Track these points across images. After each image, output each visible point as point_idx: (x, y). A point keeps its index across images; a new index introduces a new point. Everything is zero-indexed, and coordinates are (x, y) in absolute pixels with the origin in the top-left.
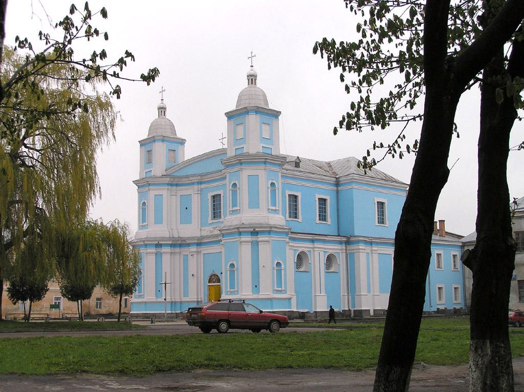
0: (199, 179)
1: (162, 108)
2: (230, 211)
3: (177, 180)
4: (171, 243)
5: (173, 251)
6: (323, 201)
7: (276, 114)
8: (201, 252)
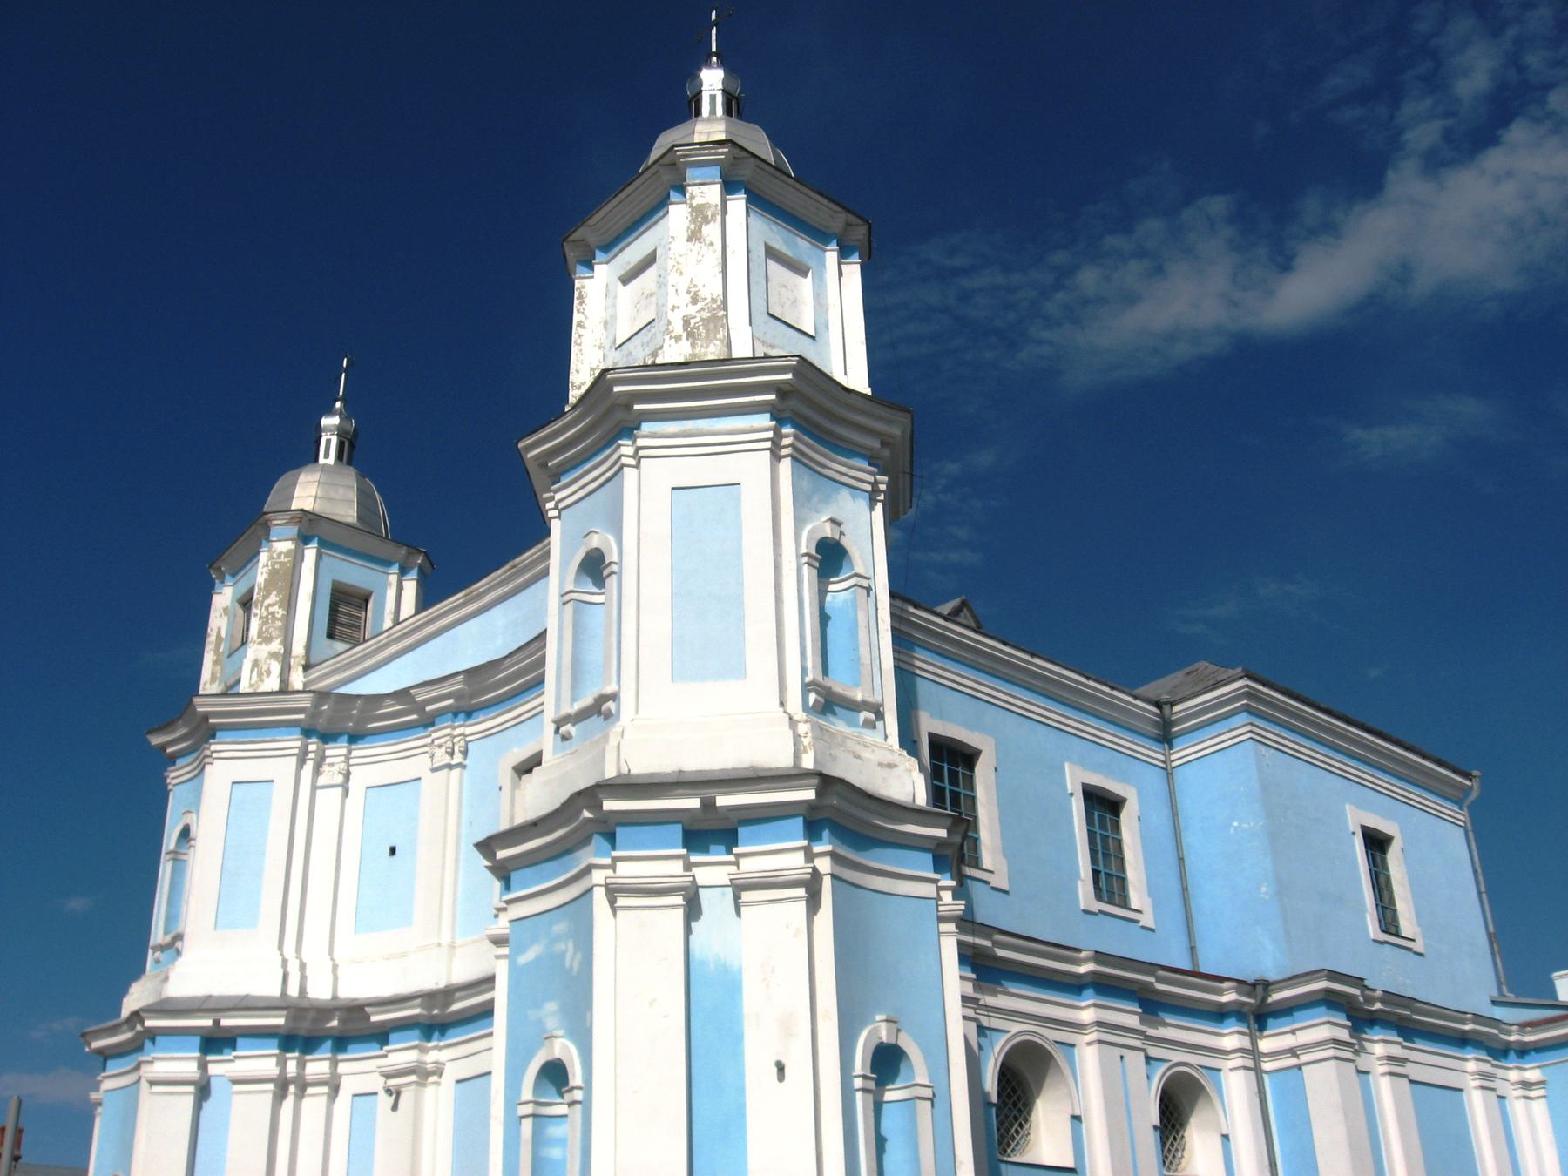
8: (439, 1072)
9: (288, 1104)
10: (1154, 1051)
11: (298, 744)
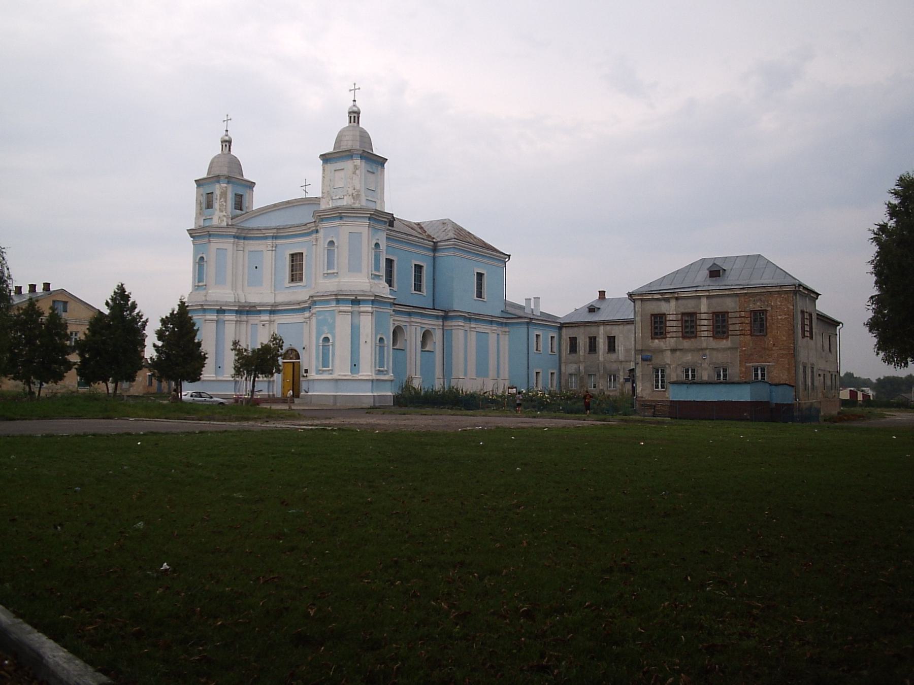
0: (274, 233)
1: (226, 141)
2: (324, 274)
3: (246, 231)
4: (237, 308)
5: (239, 319)
6: (418, 268)
7: (381, 161)
9: (238, 325)
10: (422, 326)
11: (233, 240)
